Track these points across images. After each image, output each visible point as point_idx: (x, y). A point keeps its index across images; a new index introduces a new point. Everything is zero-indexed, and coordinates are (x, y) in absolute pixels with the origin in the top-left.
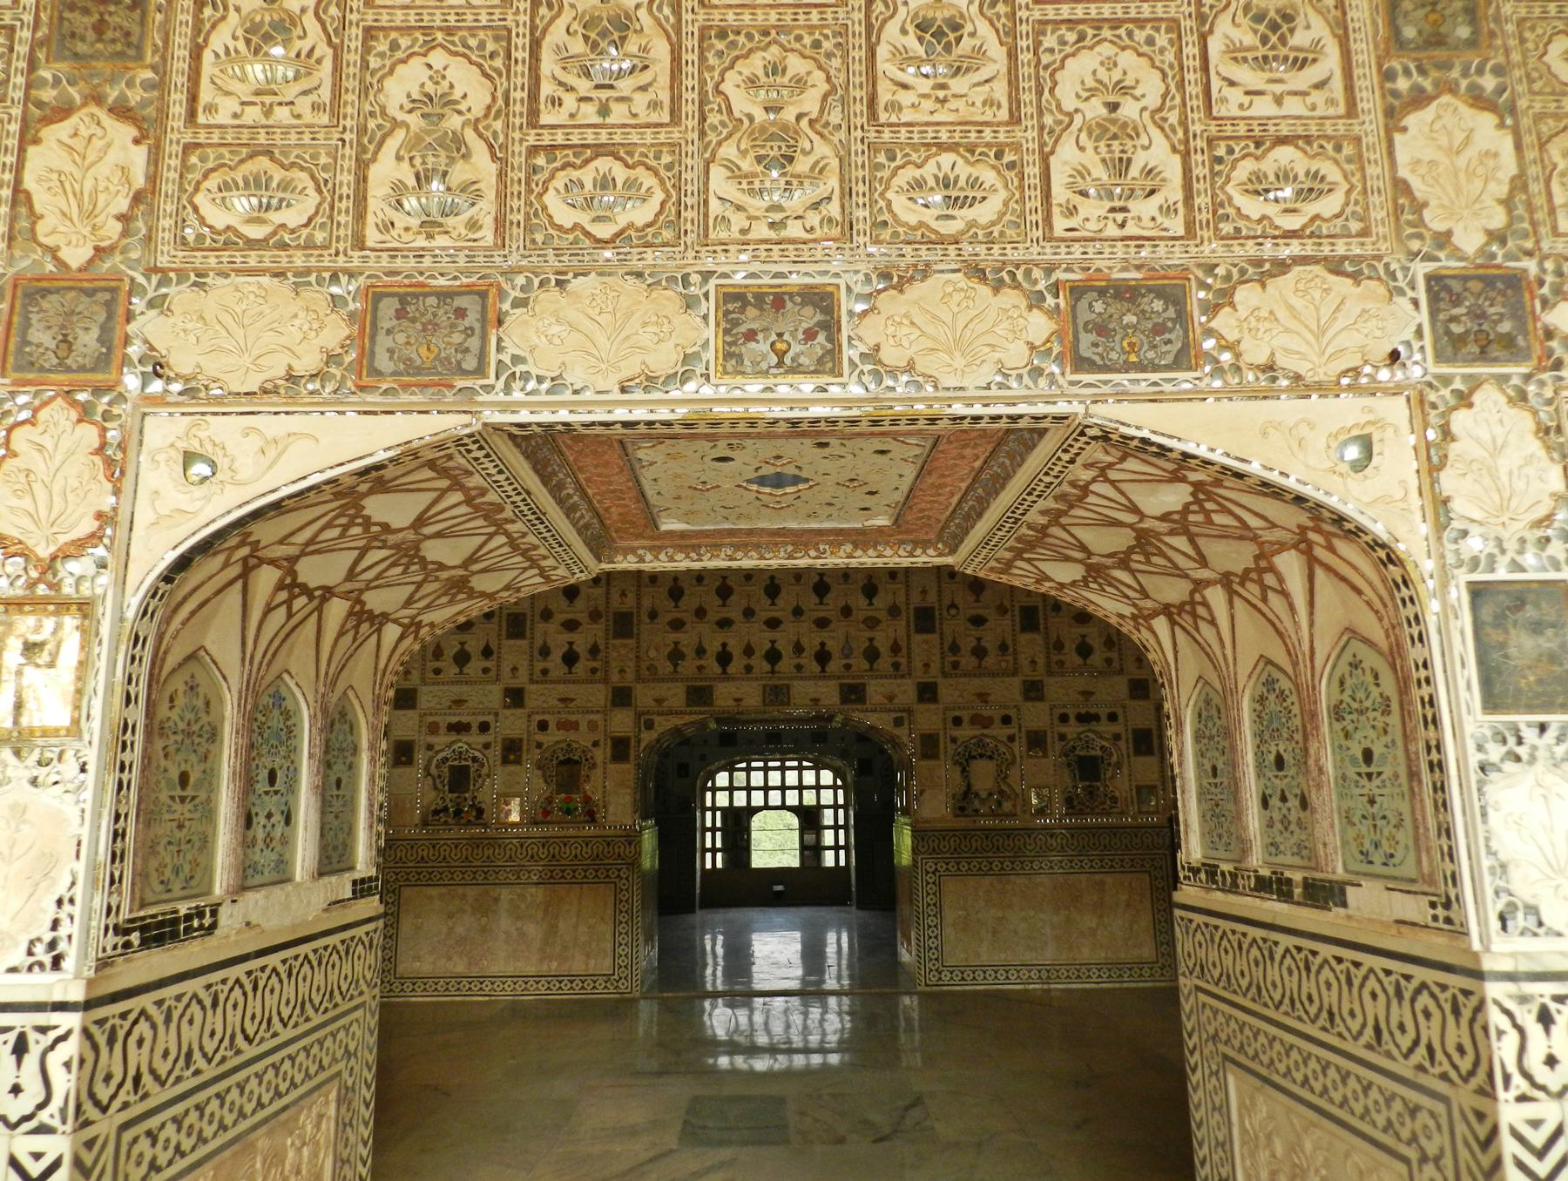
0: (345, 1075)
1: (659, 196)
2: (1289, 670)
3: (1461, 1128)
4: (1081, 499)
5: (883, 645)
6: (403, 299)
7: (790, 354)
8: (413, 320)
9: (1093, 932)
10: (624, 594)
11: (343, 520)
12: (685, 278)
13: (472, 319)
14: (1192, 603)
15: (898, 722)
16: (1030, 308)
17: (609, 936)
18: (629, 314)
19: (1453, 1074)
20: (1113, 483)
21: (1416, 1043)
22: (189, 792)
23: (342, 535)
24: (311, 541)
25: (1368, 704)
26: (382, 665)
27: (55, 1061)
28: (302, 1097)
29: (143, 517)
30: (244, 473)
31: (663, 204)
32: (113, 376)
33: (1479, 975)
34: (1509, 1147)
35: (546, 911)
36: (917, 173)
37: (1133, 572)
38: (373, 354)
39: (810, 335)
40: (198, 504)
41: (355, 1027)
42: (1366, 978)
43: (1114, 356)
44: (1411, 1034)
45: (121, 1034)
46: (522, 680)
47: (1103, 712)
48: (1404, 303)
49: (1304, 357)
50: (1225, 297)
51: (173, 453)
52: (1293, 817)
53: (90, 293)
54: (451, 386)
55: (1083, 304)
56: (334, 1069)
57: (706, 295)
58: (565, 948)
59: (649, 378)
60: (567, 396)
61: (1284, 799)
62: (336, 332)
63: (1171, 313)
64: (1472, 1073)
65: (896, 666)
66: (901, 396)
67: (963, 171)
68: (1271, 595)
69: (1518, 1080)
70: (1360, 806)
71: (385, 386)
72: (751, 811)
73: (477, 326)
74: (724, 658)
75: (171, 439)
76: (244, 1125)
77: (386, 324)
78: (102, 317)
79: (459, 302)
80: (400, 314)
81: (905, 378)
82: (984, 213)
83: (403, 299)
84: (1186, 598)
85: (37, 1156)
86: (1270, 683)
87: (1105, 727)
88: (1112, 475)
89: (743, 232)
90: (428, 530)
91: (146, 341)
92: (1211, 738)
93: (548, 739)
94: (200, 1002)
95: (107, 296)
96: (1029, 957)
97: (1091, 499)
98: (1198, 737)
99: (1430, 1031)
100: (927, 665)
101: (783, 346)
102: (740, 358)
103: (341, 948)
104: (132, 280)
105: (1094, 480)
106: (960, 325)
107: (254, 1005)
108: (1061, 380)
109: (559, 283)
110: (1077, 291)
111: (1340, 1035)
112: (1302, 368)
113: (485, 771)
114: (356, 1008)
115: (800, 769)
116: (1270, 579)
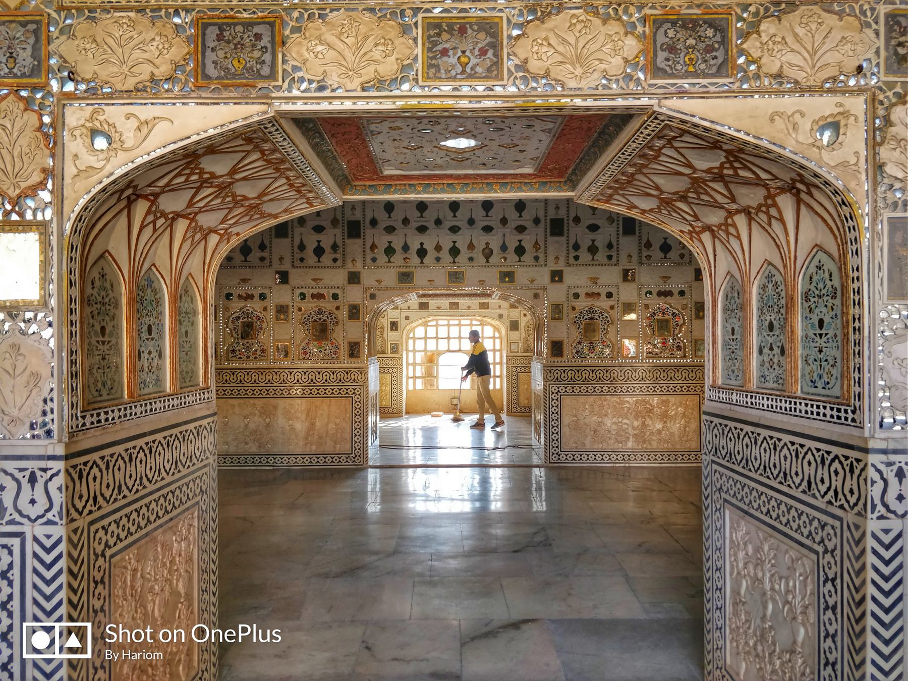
0: (201, 503)
2: (782, 270)
3: (846, 534)
4: (656, 157)
5: (528, 245)
7: (470, 65)
9: (659, 432)
11: (187, 171)
12: (403, 12)
13: (265, 41)
14: (727, 225)
15: (536, 296)
16: (626, 34)
17: (348, 430)
18: (366, 38)
19: (846, 506)
20: (676, 149)
21: (829, 489)
22: (106, 339)
23: (186, 180)
24: (168, 185)
25: (824, 291)
26: (208, 260)
27: (53, 486)
28: (178, 515)
29: (70, 170)
30: (129, 144)
32: (43, 80)
33: (866, 451)
34: (870, 543)
35: (308, 414)
37: (689, 204)
38: (204, 65)
39: (483, 52)
41: (205, 477)
42: (806, 453)
43: (679, 67)
44: (827, 484)
45: (85, 474)
46: (286, 267)
47: (676, 292)
48: (870, 33)
49: (801, 69)
50: (754, 28)
52: (776, 361)
53: (24, 24)
54: (254, 87)
55: (661, 31)
56: (195, 500)
57: (416, 24)
59: (380, 81)
60: (327, 93)
61: (771, 349)
62: (179, 50)
63: (718, 38)
64: (856, 504)
65: (536, 258)
66: (542, 95)
68: (773, 221)
69: (880, 507)
70: (814, 353)
72: (439, 353)
73: (269, 46)
74: (422, 253)
75: (82, 122)
76: (151, 527)
77: (212, 45)
78: (32, 40)
79: (257, 29)
80: (220, 38)
81: (544, 81)
84: (722, 221)
85: (48, 537)
86: (770, 277)
88: (676, 144)
90: (237, 176)
91: (61, 57)
92: (732, 311)
94: (123, 458)
95: (35, 26)
97: (662, 158)
98: (725, 310)
99: (837, 483)
100: (557, 258)
101: (466, 60)
102: (437, 67)
103: (195, 432)
104: (49, 15)
105: (664, 147)
106: (580, 45)
107: (151, 462)
108: (644, 84)
109: (320, 16)
110: (658, 23)
111: (789, 486)
112: (800, 76)
114: (205, 466)
116: (773, 212)
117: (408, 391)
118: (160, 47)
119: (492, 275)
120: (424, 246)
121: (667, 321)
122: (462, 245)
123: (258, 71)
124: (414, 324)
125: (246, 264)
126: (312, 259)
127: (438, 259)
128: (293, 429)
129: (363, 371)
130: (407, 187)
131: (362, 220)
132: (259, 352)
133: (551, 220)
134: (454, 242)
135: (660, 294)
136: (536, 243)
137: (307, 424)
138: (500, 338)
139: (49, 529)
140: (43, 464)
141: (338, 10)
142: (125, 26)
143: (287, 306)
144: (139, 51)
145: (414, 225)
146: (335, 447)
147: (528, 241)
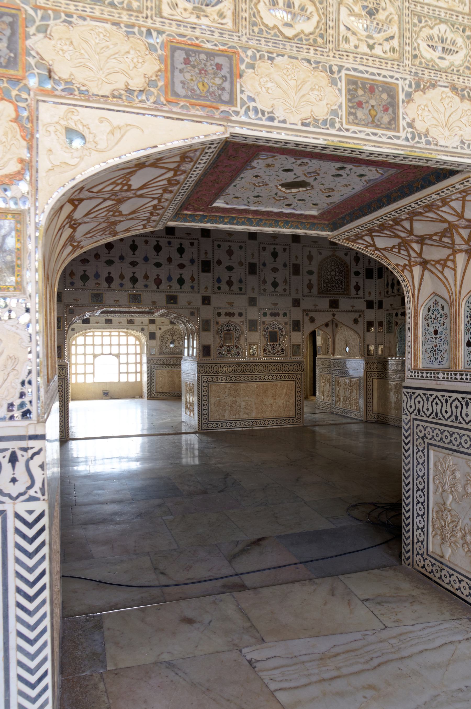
1: (315, 18)
5: (186, 277)
6: (187, 52)
8: (194, 67)
9: (271, 405)
30: (102, 145)
31: (318, 22)
36: (431, 32)
38: (173, 83)
40: (77, 160)
47: (281, 313)
51: (58, 127)
54: (217, 109)
62: (151, 66)
65: (192, 287)
67: (450, 36)
71: (182, 104)
73: (228, 75)
74: (109, 280)
75: (56, 119)
78: (8, 32)
80: (187, 61)
82: (457, 59)
83: (187, 52)
85: (30, 512)
87: (281, 319)
89: (356, 47)
96: (245, 416)
104: (26, 11)
106: (447, 115)
115: (119, 336)
118: (135, 60)
119: (161, 298)
120: (111, 275)
121: (276, 332)
122: (139, 276)
123: (220, 96)
127: (121, 285)
133: (202, 261)
134: (134, 273)
135: (272, 315)
136: (192, 276)
138: (141, 345)
139: (31, 505)
140: (24, 444)
141: (283, 56)
142: (101, 35)
144: (114, 61)
145: (103, 259)
147: (186, 275)
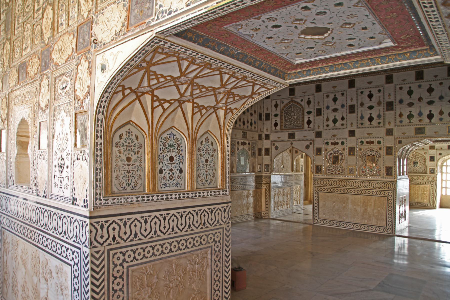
10: (389, 95)
17: (385, 215)
35: (363, 204)
58: (370, 217)
93: (363, 147)
113: (343, 158)
117: (442, 195)
120: (432, 112)
124: (446, 158)
125: (335, 127)
126: (367, 123)
127: (441, 119)
128: (356, 210)
129: (394, 183)
130: (320, 70)
131: (394, 101)
132: (341, 171)
137: (363, 209)
143: (354, 148)
145: (425, 100)
146: (377, 223)
